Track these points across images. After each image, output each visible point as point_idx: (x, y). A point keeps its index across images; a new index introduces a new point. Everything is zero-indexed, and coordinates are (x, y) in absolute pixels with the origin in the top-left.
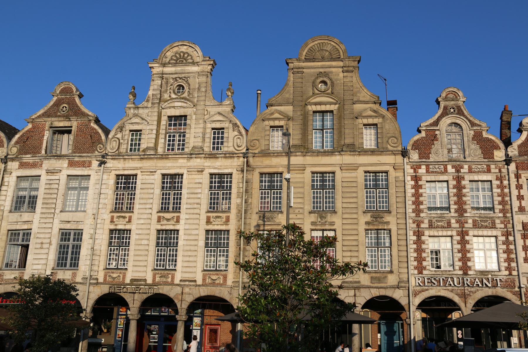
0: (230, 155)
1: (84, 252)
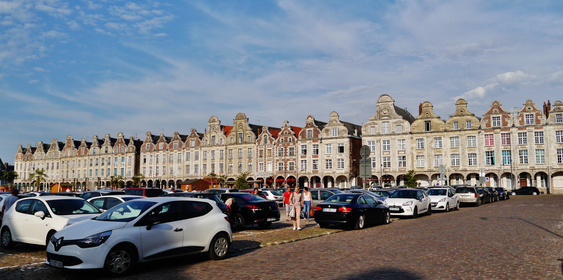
0: (223, 145)
1: (199, 170)
